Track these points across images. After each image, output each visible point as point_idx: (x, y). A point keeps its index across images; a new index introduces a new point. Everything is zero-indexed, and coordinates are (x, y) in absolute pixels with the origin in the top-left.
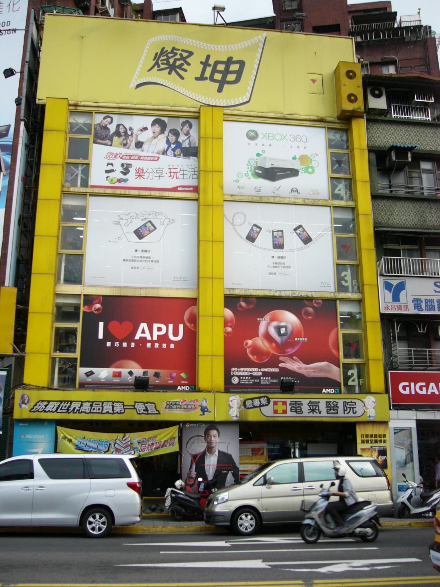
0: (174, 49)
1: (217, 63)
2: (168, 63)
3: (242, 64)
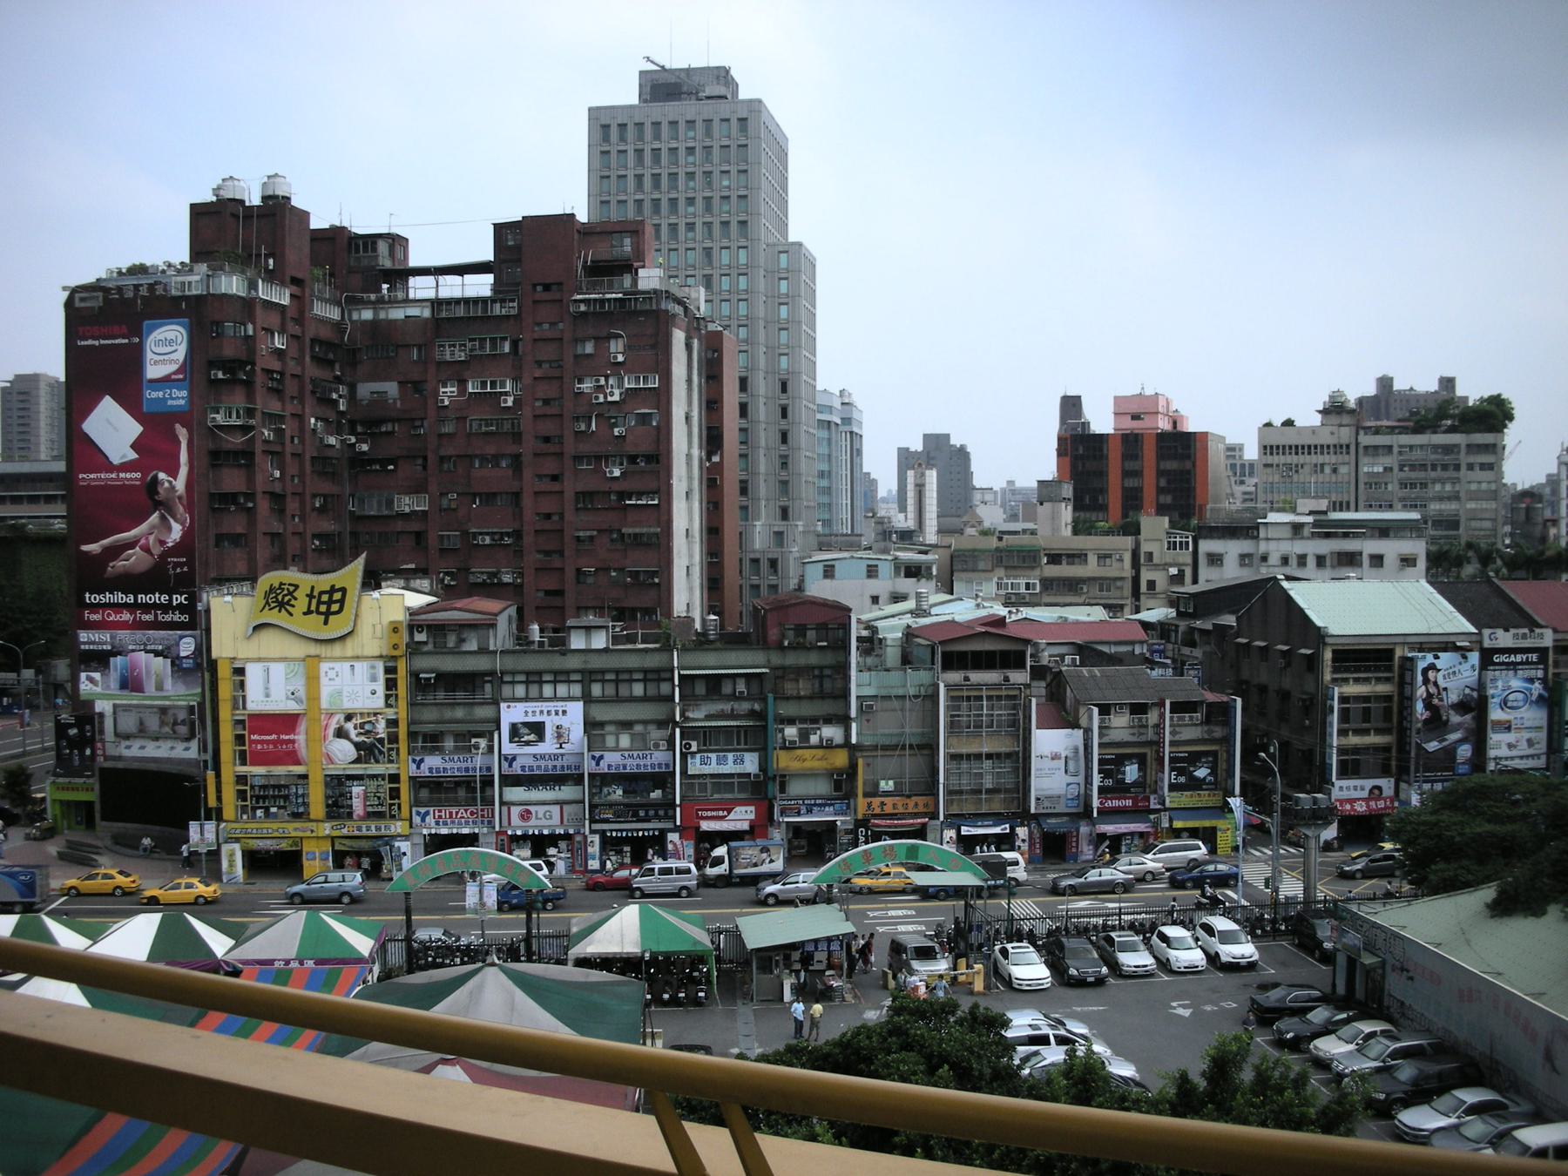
0: (281, 584)
3: (343, 590)
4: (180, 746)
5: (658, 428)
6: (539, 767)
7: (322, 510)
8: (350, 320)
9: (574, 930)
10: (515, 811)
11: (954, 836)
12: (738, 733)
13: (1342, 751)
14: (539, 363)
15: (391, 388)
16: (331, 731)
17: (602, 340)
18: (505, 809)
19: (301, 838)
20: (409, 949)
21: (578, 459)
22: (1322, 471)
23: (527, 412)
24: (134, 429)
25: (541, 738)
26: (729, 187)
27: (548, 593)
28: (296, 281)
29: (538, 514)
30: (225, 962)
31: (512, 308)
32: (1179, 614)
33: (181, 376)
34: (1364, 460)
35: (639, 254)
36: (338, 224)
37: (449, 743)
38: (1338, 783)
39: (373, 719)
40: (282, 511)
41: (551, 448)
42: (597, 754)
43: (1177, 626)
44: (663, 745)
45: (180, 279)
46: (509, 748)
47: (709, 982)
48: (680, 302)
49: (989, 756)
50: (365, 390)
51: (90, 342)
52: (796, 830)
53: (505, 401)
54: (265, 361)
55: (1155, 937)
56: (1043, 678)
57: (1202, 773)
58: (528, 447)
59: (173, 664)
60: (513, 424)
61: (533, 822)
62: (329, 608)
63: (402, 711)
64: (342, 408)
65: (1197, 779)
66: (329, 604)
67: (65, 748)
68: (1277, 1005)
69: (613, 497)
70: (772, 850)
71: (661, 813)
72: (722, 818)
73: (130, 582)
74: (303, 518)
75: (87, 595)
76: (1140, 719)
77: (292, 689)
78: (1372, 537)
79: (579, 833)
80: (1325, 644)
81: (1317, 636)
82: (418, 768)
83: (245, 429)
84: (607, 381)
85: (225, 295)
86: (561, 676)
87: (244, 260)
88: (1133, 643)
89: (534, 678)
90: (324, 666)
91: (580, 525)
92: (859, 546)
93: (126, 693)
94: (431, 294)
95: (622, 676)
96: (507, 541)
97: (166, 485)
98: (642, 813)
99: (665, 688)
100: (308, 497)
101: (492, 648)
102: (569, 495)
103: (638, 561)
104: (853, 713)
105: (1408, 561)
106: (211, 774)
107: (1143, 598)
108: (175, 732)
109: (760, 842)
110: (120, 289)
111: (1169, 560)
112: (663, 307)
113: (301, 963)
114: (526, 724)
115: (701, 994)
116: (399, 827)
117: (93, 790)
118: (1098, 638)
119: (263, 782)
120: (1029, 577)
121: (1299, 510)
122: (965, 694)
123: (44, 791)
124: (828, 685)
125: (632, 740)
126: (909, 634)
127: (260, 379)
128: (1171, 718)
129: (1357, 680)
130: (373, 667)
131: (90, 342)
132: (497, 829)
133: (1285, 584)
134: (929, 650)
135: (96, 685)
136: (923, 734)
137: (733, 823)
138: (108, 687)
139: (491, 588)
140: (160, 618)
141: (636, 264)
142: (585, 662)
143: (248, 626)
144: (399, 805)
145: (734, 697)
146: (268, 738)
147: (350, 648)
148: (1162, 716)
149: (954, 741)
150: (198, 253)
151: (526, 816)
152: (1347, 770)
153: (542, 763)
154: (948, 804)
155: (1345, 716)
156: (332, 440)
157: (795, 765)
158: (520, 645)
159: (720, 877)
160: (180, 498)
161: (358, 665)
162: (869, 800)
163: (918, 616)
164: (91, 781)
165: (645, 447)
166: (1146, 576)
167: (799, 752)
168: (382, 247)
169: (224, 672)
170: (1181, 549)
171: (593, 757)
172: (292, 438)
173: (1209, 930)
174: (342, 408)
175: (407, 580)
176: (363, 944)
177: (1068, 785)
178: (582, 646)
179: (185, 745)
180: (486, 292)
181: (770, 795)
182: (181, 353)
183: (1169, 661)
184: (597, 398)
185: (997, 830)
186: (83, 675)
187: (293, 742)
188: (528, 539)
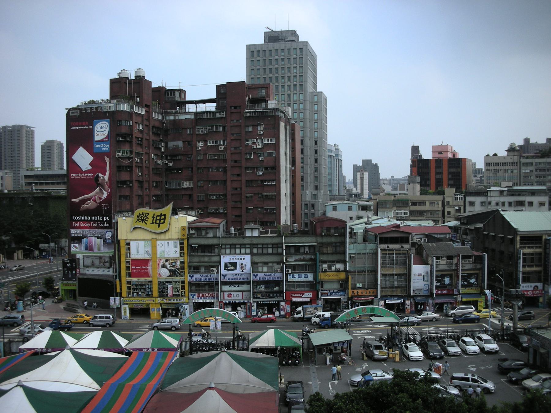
0: (143, 213)
1: (157, 216)
2: (141, 219)
3: (165, 215)
4: (106, 270)
5: (275, 157)
6: (235, 278)
7: (156, 187)
8: (166, 119)
9: (250, 338)
10: (226, 294)
11: (383, 304)
12: (306, 266)
13: (524, 273)
14: (233, 134)
15: (180, 144)
16: (160, 265)
17: (255, 126)
18: (222, 293)
19: (150, 303)
20: (191, 343)
21: (247, 168)
22: (508, 172)
23: (228, 152)
24: (90, 158)
25: (235, 268)
26: (296, 73)
27: (236, 216)
28: (147, 106)
29: (232, 188)
30: (126, 349)
31: (223, 115)
32: (461, 223)
33: (107, 140)
34: (523, 168)
35: (268, 96)
36: (161, 86)
37: (203, 270)
38: (522, 285)
39: (175, 261)
40: (142, 187)
41: (236, 164)
42: (255, 274)
44: (279, 271)
45: (106, 105)
46: (224, 272)
47: (300, 357)
48: (282, 112)
49: (396, 275)
50: (171, 144)
51: (75, 128)
52: (326, 301)
53: (221, 148)
54: (136, 134)
55: (460, 341)
56: (415, 247)
57: (472, 281)
58: (229, 164)
59: (104, 241)
60: (224, 156)
61: (232, 298)
62: (160, 221)
63: (186, 258)
64: (163, 151)
65: (471, 283)
66: (160, 220)
67: (66, 271)
68: (508, 367)
69: (259, 182)
70: (319, 308)
71: (278, 295)
72: (300, 297)
73: (89, 212)
74: (149, 189)
75: (74, 217)
76: (450, 262)
77: (147, 250)
78: (529, 195)
79: (249, 302)
80: (517, 234)
81: (514, 231)
82: (192, 278)
83: (129, 158)
84: (257, 140)
85: (122, 111)
86: (242, 246)
87: (129, 98)
88: (446, 234)
89: (233, 247)
90: (158, 242)
91: (247, 192)
92: (345, 199)
93: (87, 251)
94: (194, 110)
95: (264, 246)
96: (221, 197)
97: (102, 178)
98: (271, 295)
99: (280, 250)
100: (151, 182)
101: (218, 236)
102: (244, 181)
103: (269, 205)
104: (347, 259)
105: (542, 204)
106: (118, 280)
107: (446, 218)
108: (104, 265)
109: (314, 305)
110: (85, 109)
111: (455, 204)
112: (277, 114)
113: (153, 350)
114: (230, 263)
115: (297, 362)
116: (184, 300)
117: (76, 286)
119: (136, 283)
120: (405, 210)
121: (502, 186)
122: (387, 252)
123: (59, 286)
124: (338, 249)
125: (268, 269)
126: (366, 231)
127: (134, 140)
128: (462, 261)
129: (529, 247)
130: (175, 243)
131: (75, 128)
132: (220, 301)
133: (502, 213)
134: (375, 236)
135: (77, 248)
136: (372, 267)
137: (304, 299)
138: (81, 249)
139: (216, 214)
140: (99, 225)
141: (267, 99)
142: (251, 241)
143: (131, 228)
144: (185, 292)
145: (304, 253)
146: (138, 268)
147: (167, 236)
148: (458, 260)
149: (383, 269)
150: (113, 95)
151: (230, 296)
152: (526, 280)
153: (236, 277)
154: (381, 292)
155: (524, 260)
156: (159, 162)
157: (327, 278)
158: (227, 235)
159: (299, 318)
160: (106, 183)
161: (170, 242)
162: (353, 290)
163: (368, 224)
164: (75, 282)
165: (271, 164)
166: (447, 209)
167: (328, 273)
168: (177, 94)
169: (123, 244)
170: (460, 200)
171: (254, 275)
172: (146, 161)
173: (480, 339)
174: (163, 151)
175: (187, 211)
176: (175, 343)
177: (424, 285)
178: (250, 235)
179: (108, 270)
180: (214, 109)
181: (317, 289)
182: (107, 132)
183: (459, 240)
184: (253, 147)
185: (399, 301)
186: (72, 245)
187: (147, 269)
188: (229, 197)
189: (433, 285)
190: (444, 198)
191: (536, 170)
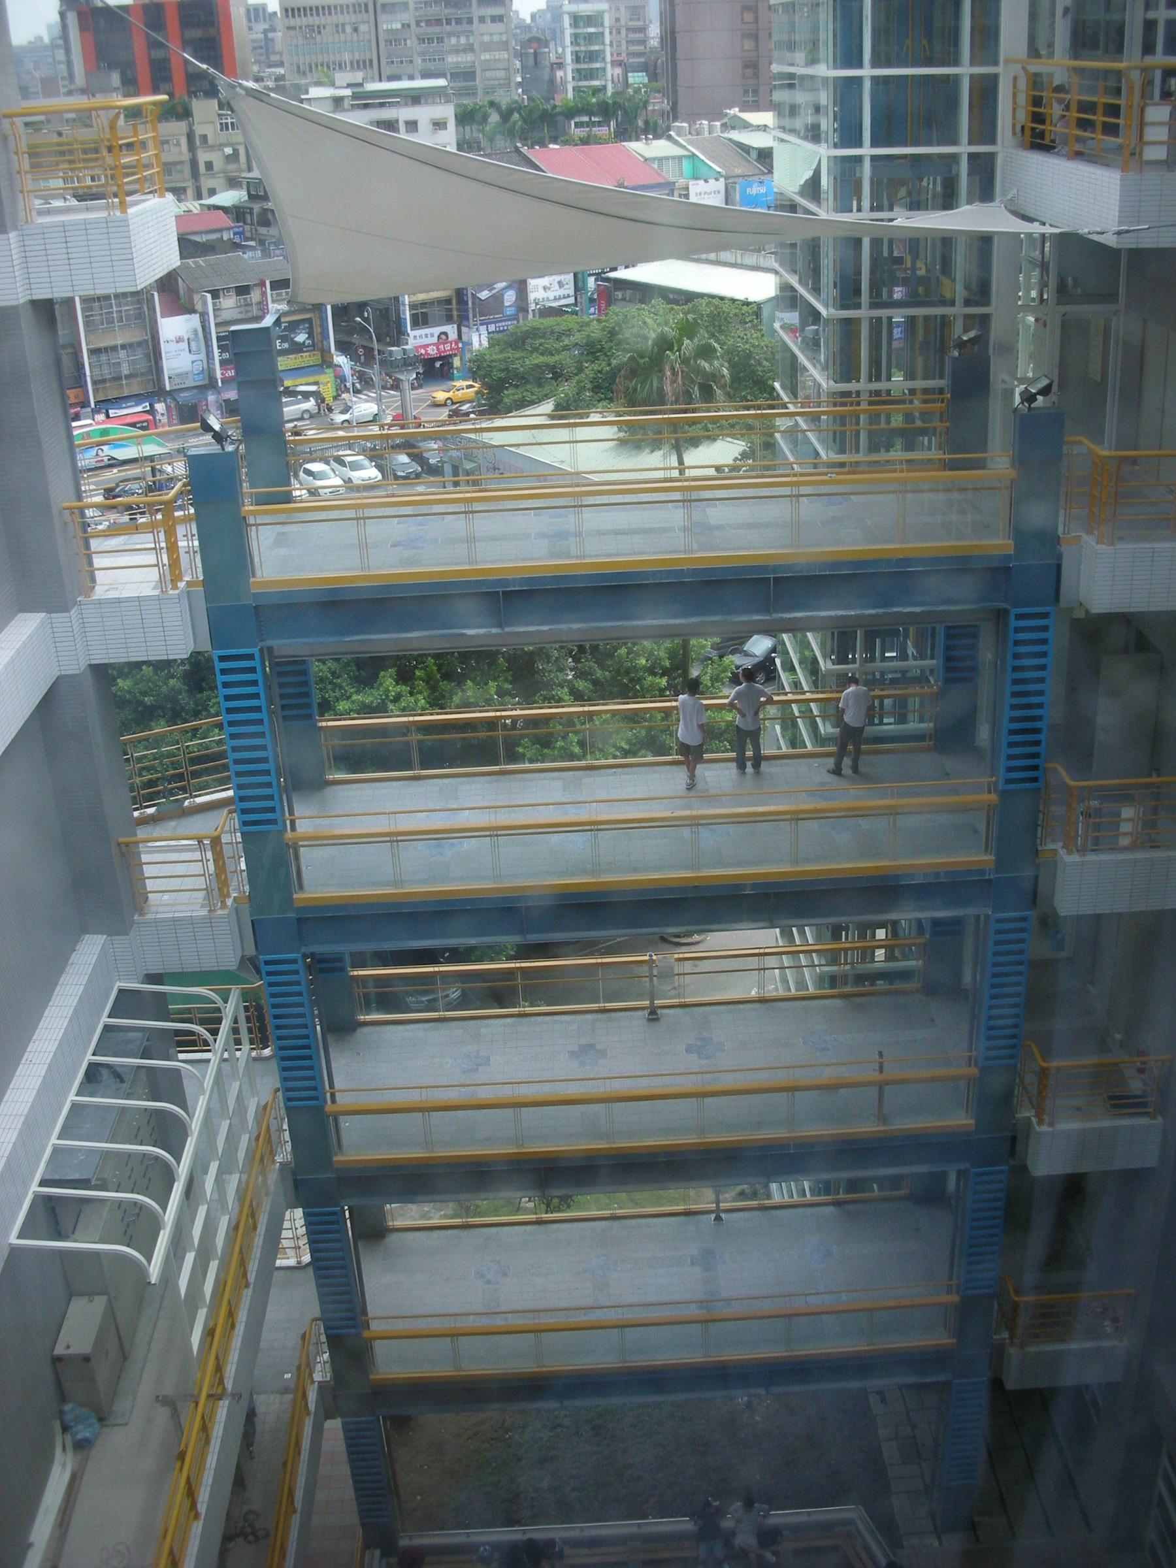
22: (344, 31)
34: (382, 18)
38: (412, 333)
43: (252, 209)
49: (123, 347)
55: (301, 474)
57: (301, 338)
65: (297, 343)
76: (245, 299)
78: (406, 105)
88: (220, 230)
107: (202, 179)
111: (222, 140)
118: (190, 230)
121: (337, 83)
148: (264, 294)
152: (420, 320)
154: (96, 391)
166: (203, 157)
170: (233, 129)
177: (193, 362)
183: (253, 243)
189: (213, 359)
190: (190, 126)
191: (418, 23)
